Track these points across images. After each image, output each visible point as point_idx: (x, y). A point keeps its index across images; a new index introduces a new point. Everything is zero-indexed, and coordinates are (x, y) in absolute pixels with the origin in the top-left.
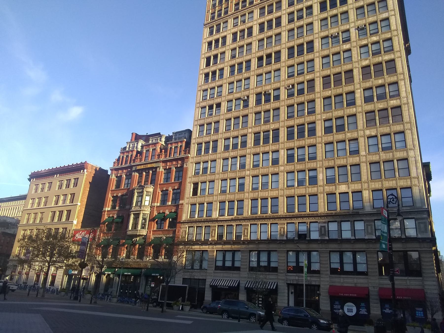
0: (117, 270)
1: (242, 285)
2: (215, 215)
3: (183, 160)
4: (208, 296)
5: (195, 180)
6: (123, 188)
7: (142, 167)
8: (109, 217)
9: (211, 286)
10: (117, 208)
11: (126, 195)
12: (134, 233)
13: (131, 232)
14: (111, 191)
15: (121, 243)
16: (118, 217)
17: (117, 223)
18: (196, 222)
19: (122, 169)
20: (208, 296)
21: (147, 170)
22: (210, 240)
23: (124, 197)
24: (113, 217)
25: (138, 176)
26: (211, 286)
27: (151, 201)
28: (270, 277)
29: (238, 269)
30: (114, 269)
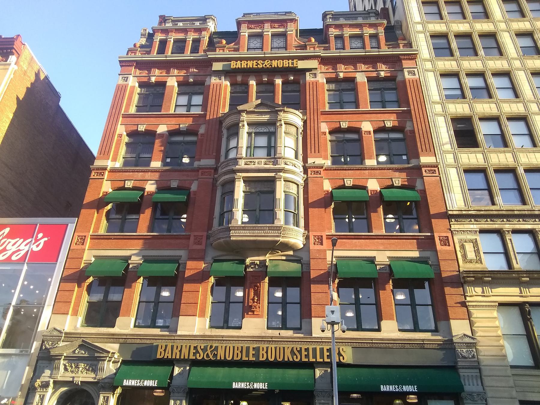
0: (177, 370)
3: (395, 61)
6: (172, 112)
8: (123, 188)
10: (156, 164)
11: (190, 132)
12: (262, 234)
13: (242, 233)
14: (125, 116)
15: (188, 274)
16: (160, 189)
17: (155, 205)
19: (166, 66)
21: (265, 74)
25: (229, 89)
30: (168, 369)
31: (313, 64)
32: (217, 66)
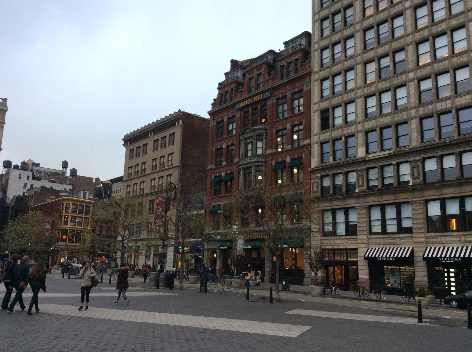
1: (419, 255)
2: (361, 153)
4: (364, 274)
5: (324, 105)
7: (247, 102)
9: (366, 258)
18: (332, 167)
20: (364, 274)
22: (357, 191)
23: (231, 148)
24: (220, 176)
26: (366, 258)
27: (264, 148)
28: (467, 239)
29: (409, 230)
31: (268, 94)
32: (237, 107)
